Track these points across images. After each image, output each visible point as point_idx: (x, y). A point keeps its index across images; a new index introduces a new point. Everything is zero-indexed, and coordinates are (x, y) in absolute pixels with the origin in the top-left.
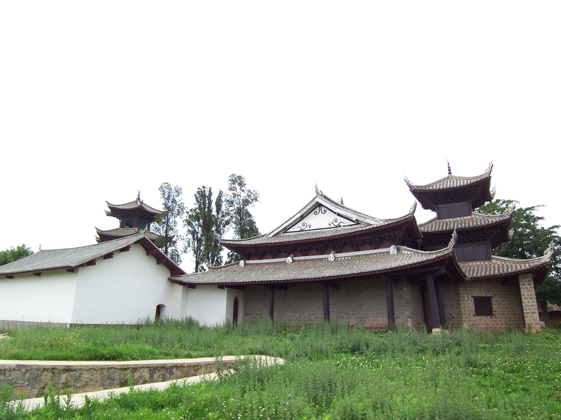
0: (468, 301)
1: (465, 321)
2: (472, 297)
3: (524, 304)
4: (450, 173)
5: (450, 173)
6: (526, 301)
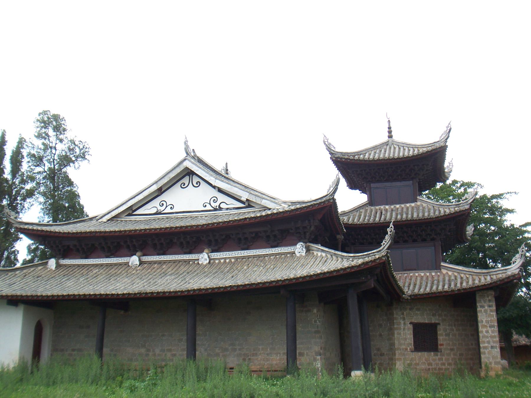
0: (404, 329)
1: (400, 359)
2: (410, 323)
3: (481, 335)
4: (390, 137)
5: (390, 137)
6: (484, 330)
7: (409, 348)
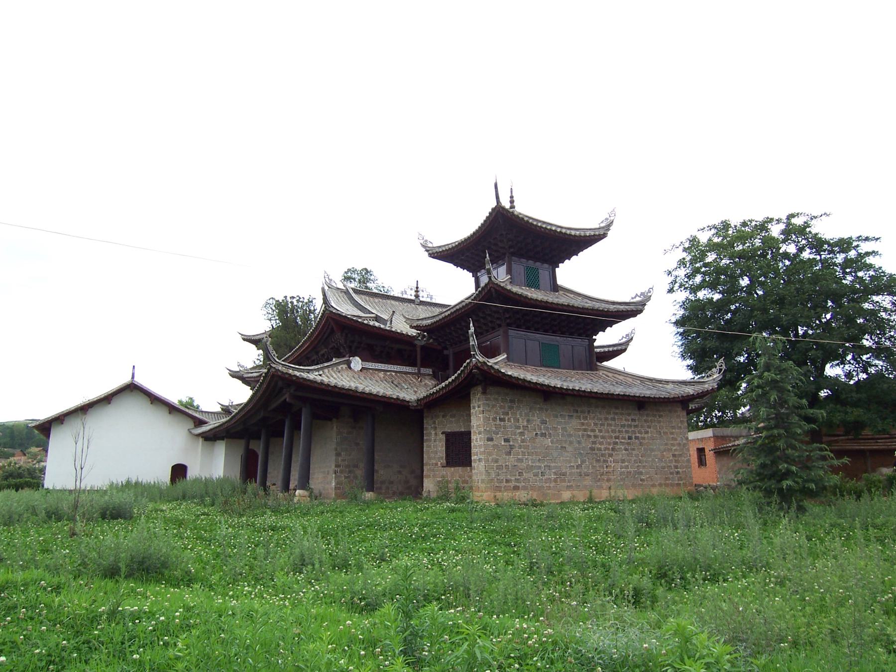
1: (429, 476)
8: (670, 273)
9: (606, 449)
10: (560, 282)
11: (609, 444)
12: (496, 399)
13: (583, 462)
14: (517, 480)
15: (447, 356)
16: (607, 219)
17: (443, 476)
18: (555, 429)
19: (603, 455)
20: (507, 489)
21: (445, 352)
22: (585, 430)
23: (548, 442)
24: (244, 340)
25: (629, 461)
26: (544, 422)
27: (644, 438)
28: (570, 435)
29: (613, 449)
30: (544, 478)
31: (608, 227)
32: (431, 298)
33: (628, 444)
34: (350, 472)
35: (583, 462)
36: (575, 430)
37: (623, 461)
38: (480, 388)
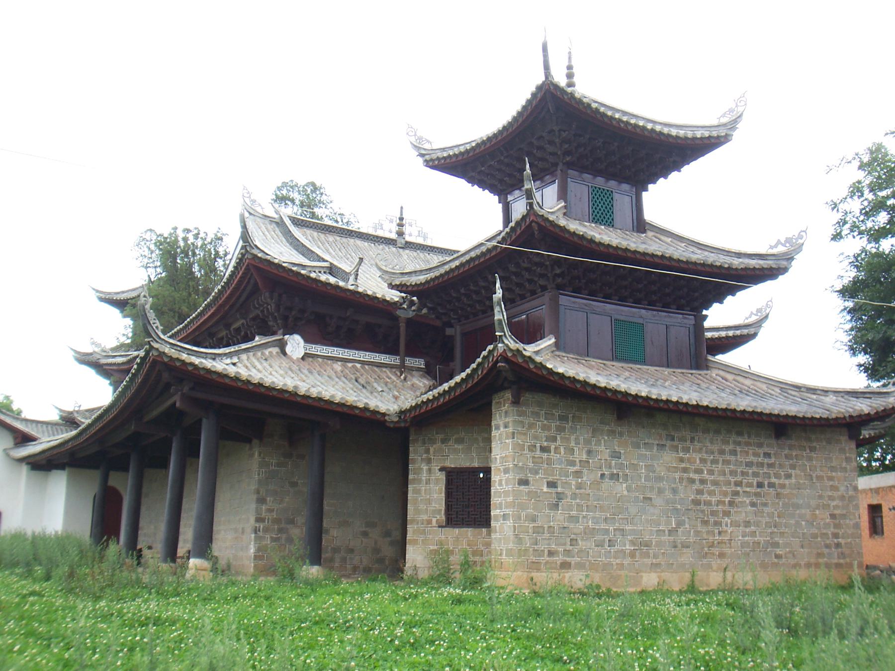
0: (428, 482)
1: (415, 542)
2: (441, 470)
7: (434, 520)
8: (835, 206)
9: (719, 502)
10: (649, 215)
11: (725, 494)
12: (537, 415)
13: (680, 524)
14: (567, 553)
15: (451, 338)
16: (731, 111)
17: (441, 543)
18: (635, 467)
19: (714, 513)
20: (550, 566)
21: (449, 331)
22: (685, 470)
23: (621, 488)
24: (102, 300)
25: (757, 524)
26: (616, 455)
27: (783, 486)
28: (660, 479)
29: (731, 503)
30: (613, 549)
31: (733, 125)
32: (425, 238)
33: (757, 495)
34: (280, 530)
35: (680, 524)
36: (668, 469)
37: (747, 524)
38: (508, 395)
